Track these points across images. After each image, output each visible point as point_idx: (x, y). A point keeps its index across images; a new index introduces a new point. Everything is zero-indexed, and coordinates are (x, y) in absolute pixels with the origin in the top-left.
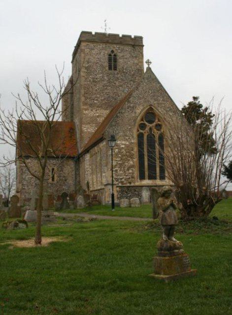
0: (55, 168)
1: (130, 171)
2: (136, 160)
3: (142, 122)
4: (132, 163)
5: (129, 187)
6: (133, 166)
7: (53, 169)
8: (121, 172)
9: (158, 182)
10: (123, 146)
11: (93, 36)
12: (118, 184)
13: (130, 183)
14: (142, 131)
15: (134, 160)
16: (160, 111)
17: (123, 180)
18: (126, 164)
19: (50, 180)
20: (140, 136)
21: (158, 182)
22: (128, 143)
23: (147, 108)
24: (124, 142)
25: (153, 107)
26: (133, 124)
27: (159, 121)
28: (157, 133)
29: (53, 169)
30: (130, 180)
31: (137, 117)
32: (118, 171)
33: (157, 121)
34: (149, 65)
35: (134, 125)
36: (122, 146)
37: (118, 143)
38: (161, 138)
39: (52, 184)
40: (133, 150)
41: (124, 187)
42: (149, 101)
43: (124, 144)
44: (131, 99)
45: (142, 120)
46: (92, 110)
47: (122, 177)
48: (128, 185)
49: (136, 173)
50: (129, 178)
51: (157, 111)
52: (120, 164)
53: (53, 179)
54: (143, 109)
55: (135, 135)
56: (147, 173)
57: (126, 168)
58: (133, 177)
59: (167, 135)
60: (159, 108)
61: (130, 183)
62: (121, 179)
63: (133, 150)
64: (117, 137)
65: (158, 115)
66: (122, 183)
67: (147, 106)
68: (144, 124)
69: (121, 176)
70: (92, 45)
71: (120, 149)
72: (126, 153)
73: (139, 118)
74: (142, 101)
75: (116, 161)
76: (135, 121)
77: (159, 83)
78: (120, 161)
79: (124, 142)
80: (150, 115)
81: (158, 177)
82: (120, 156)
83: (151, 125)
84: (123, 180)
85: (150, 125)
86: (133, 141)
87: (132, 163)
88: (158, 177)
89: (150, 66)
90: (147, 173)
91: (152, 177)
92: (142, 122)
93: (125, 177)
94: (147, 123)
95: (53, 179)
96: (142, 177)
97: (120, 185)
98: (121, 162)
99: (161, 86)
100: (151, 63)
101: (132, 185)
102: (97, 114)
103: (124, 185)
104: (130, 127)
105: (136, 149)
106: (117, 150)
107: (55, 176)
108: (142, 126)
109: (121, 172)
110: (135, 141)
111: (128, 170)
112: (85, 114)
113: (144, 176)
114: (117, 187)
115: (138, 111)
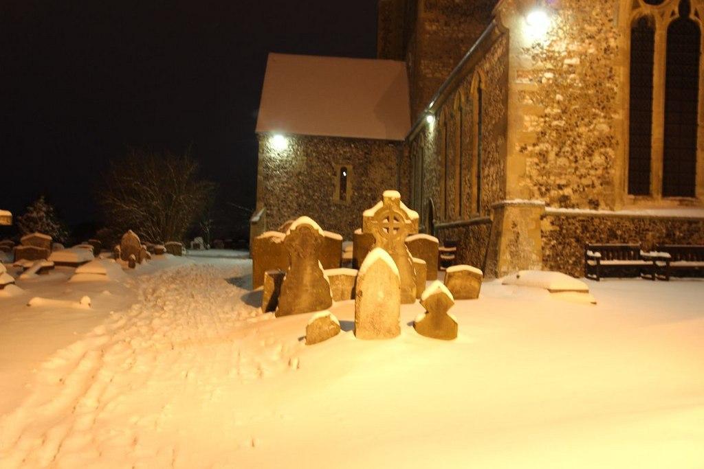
1: (598, 159)
2: (621, 116)
4: (605, 128)
6: (606, 141)
8: (562, 161)
10: (575, 61)
15: (616, 116)
19: (336, 197)
30: (593, 194)
32: (552, 156)
36: (567, 61)
39: (339, 207)
46: (446, 24)
47: (563, 182)
50: (593, 186)
52: (557, 129)
57: (581, 148)
58: (606, 182)
62: (560, 187)
72: (587, 87)
82: (559, 97)
87: (605, 128)
95: (342, 198)
98: (562, 123)
102: (461, 35)
105: (622, 73)
106: (549, 75)
110: (620, 41)
111: (589, 153)
112: (428, 33)
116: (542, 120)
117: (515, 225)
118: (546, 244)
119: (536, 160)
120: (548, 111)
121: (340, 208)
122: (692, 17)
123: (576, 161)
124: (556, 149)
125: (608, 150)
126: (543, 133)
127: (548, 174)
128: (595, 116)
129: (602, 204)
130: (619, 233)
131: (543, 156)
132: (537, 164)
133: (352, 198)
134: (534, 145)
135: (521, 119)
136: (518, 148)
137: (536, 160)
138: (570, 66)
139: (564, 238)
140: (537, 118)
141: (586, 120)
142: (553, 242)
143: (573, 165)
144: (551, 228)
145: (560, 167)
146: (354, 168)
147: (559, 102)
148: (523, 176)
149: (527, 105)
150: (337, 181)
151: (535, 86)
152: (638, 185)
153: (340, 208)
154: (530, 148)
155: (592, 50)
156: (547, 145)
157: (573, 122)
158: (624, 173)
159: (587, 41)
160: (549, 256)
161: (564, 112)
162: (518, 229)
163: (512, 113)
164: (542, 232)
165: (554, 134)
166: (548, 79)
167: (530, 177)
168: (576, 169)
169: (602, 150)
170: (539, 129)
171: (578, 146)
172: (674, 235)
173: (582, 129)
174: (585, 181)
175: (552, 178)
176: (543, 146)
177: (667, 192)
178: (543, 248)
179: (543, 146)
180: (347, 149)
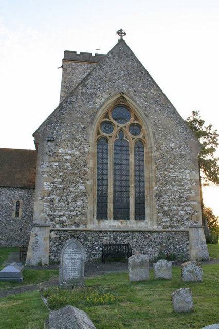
0: (21, 201)
1: (79, 203)
3: (108, 120)
4: (83, 188)
5: (76, 231)
6: (84, 194)
7: (18, 202)
8: (62, 204)
9: (132, 224)
10: (69, 157)
11: (78, 55)
12: (54, 226)
13: (78, 225)
14: (105, 134)
15: (88, 182)
16: (137, 103)
17: (64, 218)
18: (72, 189)
19: (14, 215)
20: (102, 142)
21: (132, 224)
22: (77, 153)
23: (115, 98)
24: (70, 151)
25: (125, 96)
26: (90, 120)
27: (136, 118)
28: (131, 139)
29: (18, 202)
30: (77, 220)
31: (98, 109)
33: (132, 118)
34: (122, 37)
35: (92, 122)
36: (65, 157)
37: (60, 151)
38: (140, 144)
40: (85, 165)
41: (64, 231)
42: (118, 87)
43: (71, 155)
44: (89, 82)
45: (107, 116)
47: (62, 214)
48: (74, 228)
49: (91, 206)
50: (77, 216)
51: (134, 103)
53: (17, 214)
54: (107, 99)
55: (92, 139)
56: (110, 206)
57: (71, 197)
59: (150, 141)
60: (137, 99)
61: (78, 225)
62: (60, 216)
63: (85, 165)
64: (59, 141)
65: (134, 110)
66: (62, 223)
67: (115, 95)
68: (110, 123)
69: (60, 211)
70: (75, 64)
71: (62, 162)
73: (101, 113)
74: (108, 85)
75: (54, 182)
76: (93, 116)
77: (137, 61)
78: (60, 183)
79: (70, 151)
80: (121, 107)
81: (132, 216)
82: (61, 174)
83: (122, 126)
84: (64, 218)
85: (119, 125)
86: (86, 150)
87: (83, 188)
88: (132, 216)
89: (124, 38)
90: (110, 206)
91: (121, 213)
92: (108, 120)
93: (68, 213)
94: (114, 122)
95: (17, 214)
96: (102, 214)
97: (58, 227)
99: (141, 66)
100: (125, 34)
101: (81, 228)
103: (65, 229)
104: (82, 126)
105: (92, 163)
106: (57, 164)
107: (20, 210)
108: (107, 125)
109: (62, 204)
110: (91, 148)
111: (75, 200)
113: (128, 214)
114: (51, 231)
115: (99, 101)
116: (52, 184)
117: (36, 235)
118: (52, 244)
119: (49, 204)
120: (55, 180)
121: (15, 221)
122: (124, 138)
123: (68, 204)
124: (59, 198)
125: (84, 198)
126: (53, 191)
127: (54, 210)
128: (78, 182)
129: (81, 225)
130: (90, 238)
131: (52, 201)
132: (49, 206)
133: (21, 216)
134: (48, 196)
135: (42, 185)
136: (40, 198)
137: (49, 204)
138: (67, 160)
139: (62, 241)
140: (49, 184)
141: (74, 184)
142: (56, 243)
143: (67, 205)
144: (55, 236)
145: (61, 207)
146: (23, 201)
147: (60, 176)
148: (42, 211)
149: (45, 177)
150: (14, 208)
151: (50, 169)
152: (102, 214)
153: (15, 221)
154: (46, 198)
155: (77, 153)
156: (54, 196)
157: (67, 185)
158: (94, 207)
159: (74, 149)
160: (54, 250)
161: (63, 181)
162: (38, 237)
163: (37, 182)
164: (50, 238)
165: (58, 191)
166: (56, 166)
167: (46, 212)
168: (68, 207)
169: (81, 198)
170: (51, 189)
171: (70, 196)
172: (117, 238)
173: (72, 189)
174: (73, 214)
175: (57, 212)
176: (52, 197)
177: (115, 218)
178: (51, 246)
179: (52, 197)
180: (20, 192)
